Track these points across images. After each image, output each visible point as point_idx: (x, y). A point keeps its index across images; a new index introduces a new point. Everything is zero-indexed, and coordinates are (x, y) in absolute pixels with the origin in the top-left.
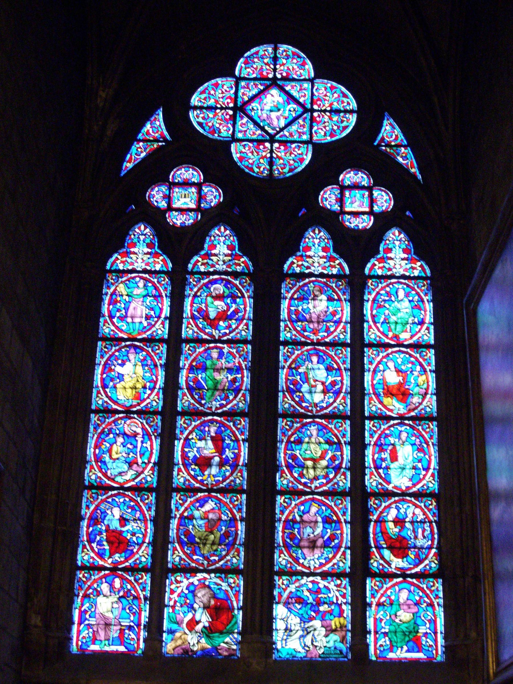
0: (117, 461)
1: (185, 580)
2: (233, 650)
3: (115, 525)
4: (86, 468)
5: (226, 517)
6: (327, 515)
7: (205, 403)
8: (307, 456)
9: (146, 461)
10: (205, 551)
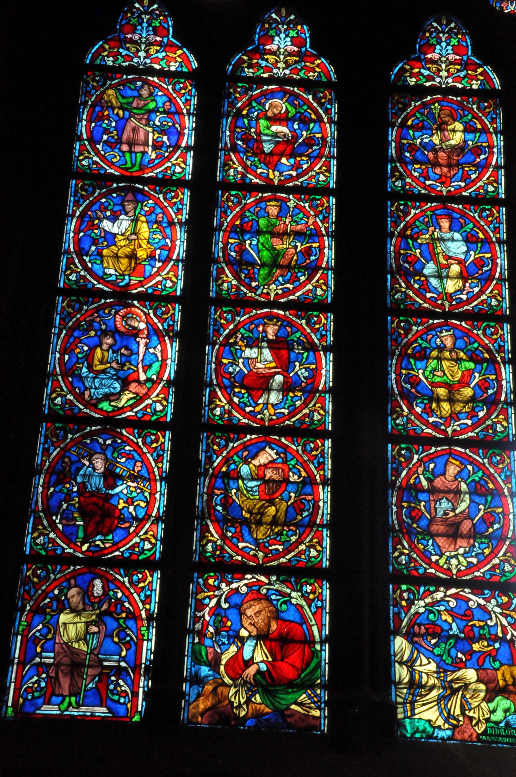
0: (103, 376)
1: (223, 585)
2: (314, 717)
3: (97, 483)
4: (47, 385)
5: (296, 477)
6: (477, 479)
7: (258, 287)
8: (438, 380)
9: (154, 377)
10: (261, 533)
